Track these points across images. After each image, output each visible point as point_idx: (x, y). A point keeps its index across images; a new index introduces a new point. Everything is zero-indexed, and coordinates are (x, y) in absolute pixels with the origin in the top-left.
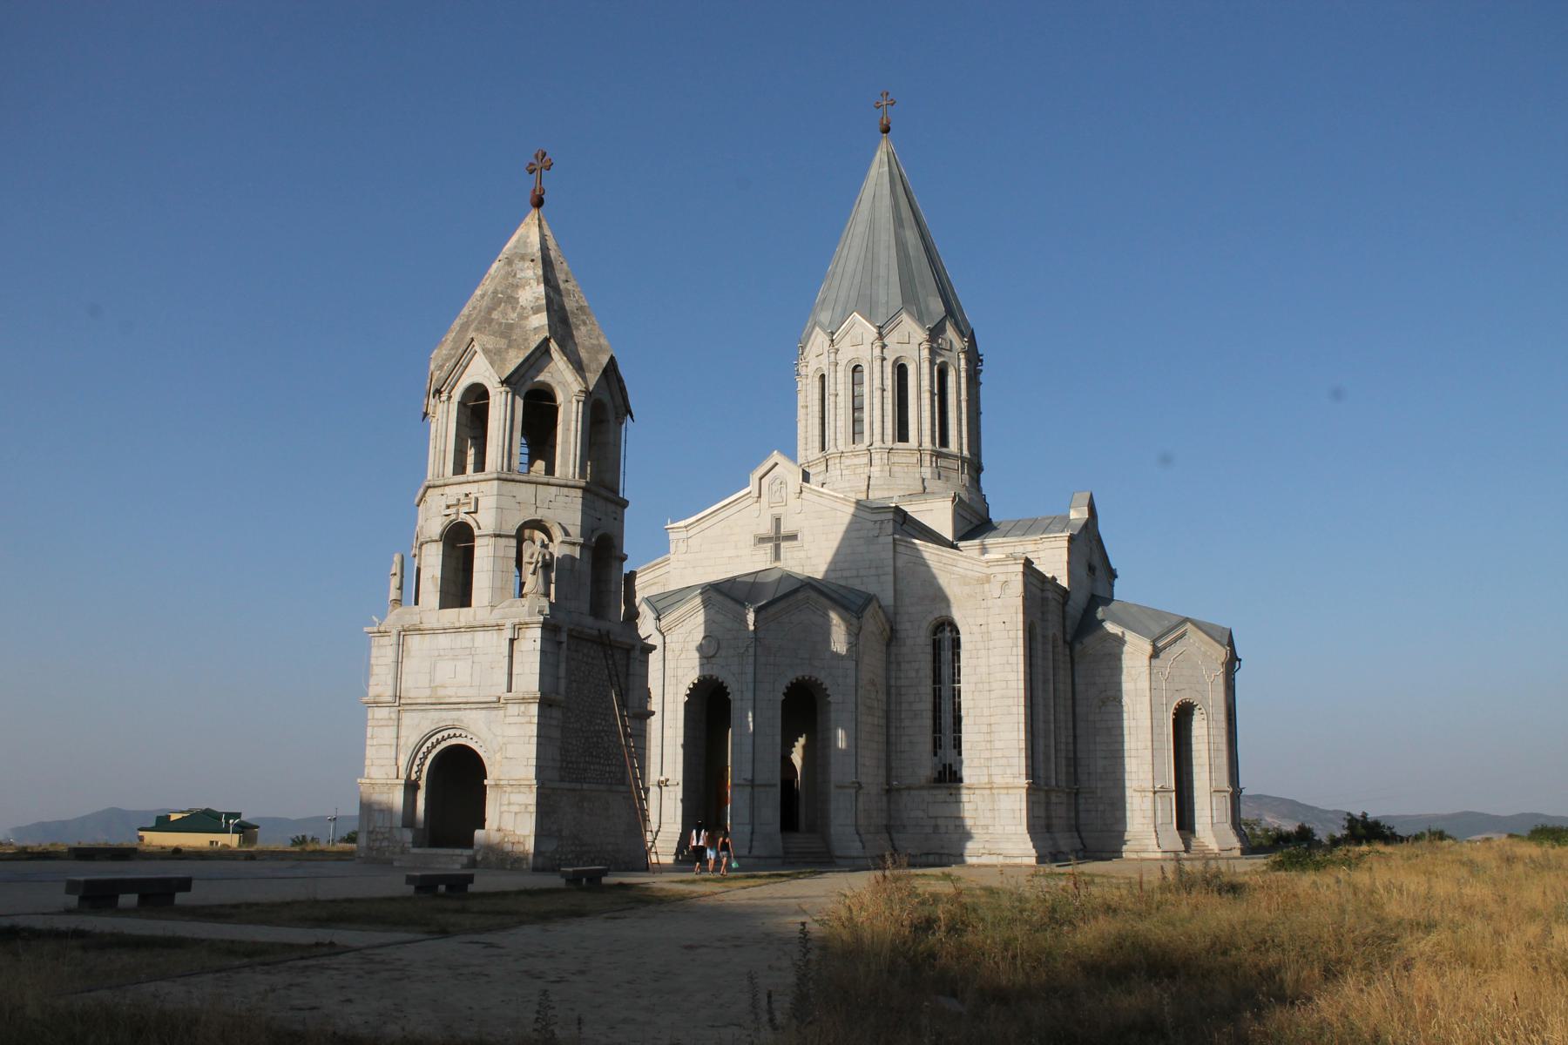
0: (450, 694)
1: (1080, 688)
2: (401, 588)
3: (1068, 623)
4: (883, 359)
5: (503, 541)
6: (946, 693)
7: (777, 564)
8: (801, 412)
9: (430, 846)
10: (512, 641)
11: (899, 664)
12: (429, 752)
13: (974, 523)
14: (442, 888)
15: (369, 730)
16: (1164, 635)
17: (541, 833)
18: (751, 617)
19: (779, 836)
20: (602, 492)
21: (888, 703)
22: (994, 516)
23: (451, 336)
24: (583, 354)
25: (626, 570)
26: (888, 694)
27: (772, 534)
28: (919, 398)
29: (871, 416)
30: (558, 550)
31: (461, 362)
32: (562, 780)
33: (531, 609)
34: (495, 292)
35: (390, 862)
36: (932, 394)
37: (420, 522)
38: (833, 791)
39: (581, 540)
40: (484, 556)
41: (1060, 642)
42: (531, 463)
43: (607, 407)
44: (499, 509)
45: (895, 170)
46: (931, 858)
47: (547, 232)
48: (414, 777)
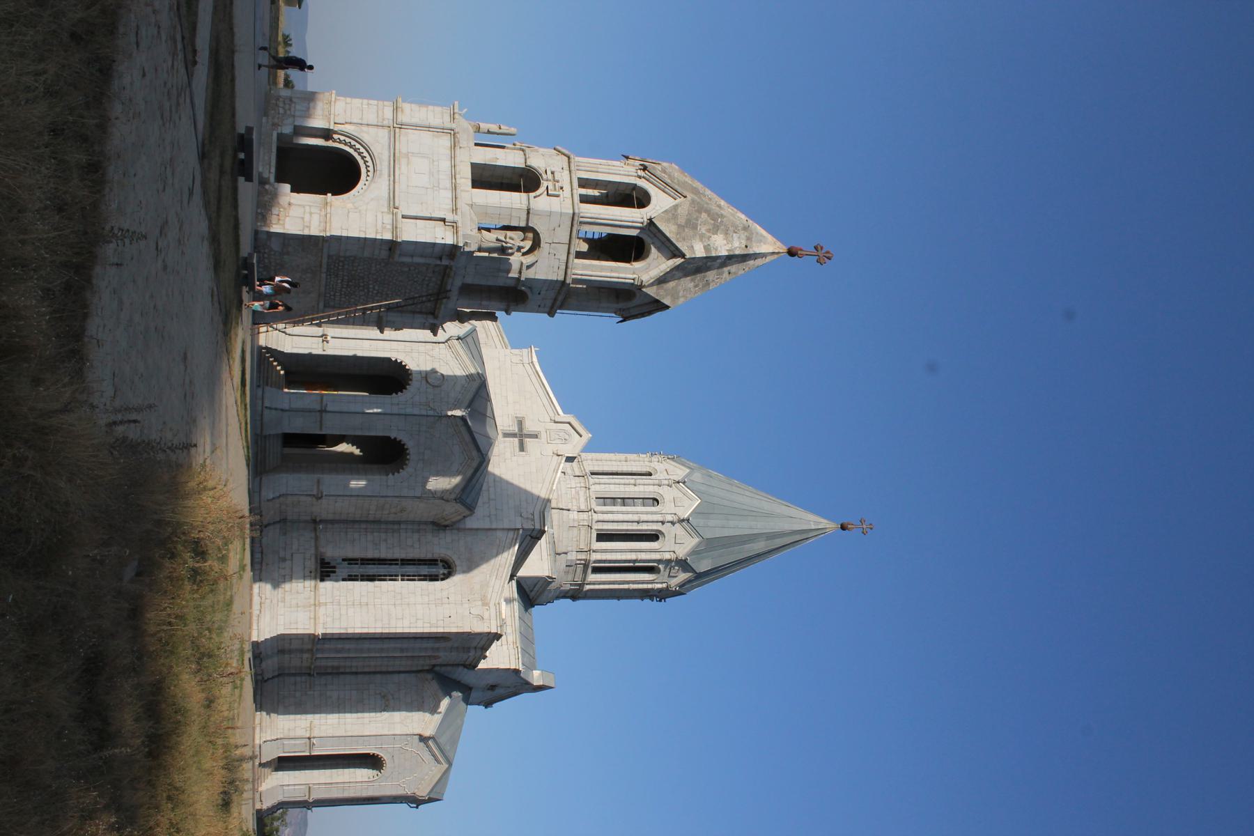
0: (402, 168)
1: (396, 677)
2: (489, 132)
3: (449, 668)
4: (663, 523)
5: (524, 216)
6: (393, 569)
7: (500, 435)
8: (622, 456)
9: (279, 150)
10: (443, 220)
11: (418, 531)
12: (355, 150)
13: (531, 594)
14: (242, 156)
15: (375, 102)
16: (438, 746)
17: (288, 240)
18: (458, 413)
19: (280, 432)
20: (562, 297)
21: (387, 522)
22: (536, 609)
23: (688, 180)
24: (671, 284)
25: (498, 314)
26: (393, 523)
27: (525, 432)
28: (631, 551)
29: (618, 512)
30: (516, 259)
31: (668, 187)
32: (329, 257)
33: (470, 237)
35: (266, 114)
36: (635, 561)
37: (542, 150)
39: (523, 279)
40: (512, 201)
41: (434, 662)
42: (586, 240)
43: (629, 302)
44: (550, 214)
45: (811, 534)
46: (258, 556)
47: (769, 259)
48: (336, 136)
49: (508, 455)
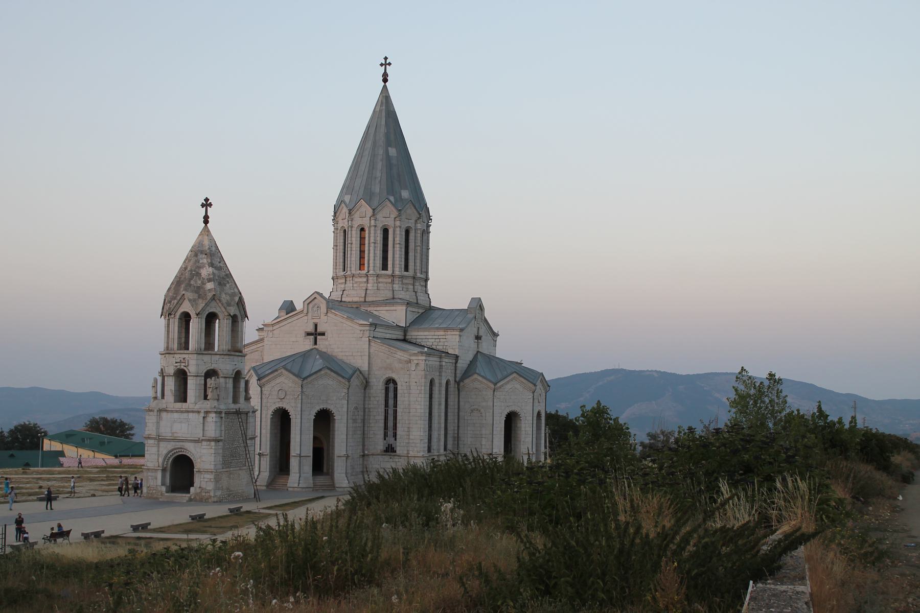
3: (458, 372)
6: (391, 412)
19: (311, 478)
26: (364, 411)
27: (313, 331)
31: (179, 304)
34: (191, 271)
40: (193, 385)
41: (452, 382)
49: (327, 343)
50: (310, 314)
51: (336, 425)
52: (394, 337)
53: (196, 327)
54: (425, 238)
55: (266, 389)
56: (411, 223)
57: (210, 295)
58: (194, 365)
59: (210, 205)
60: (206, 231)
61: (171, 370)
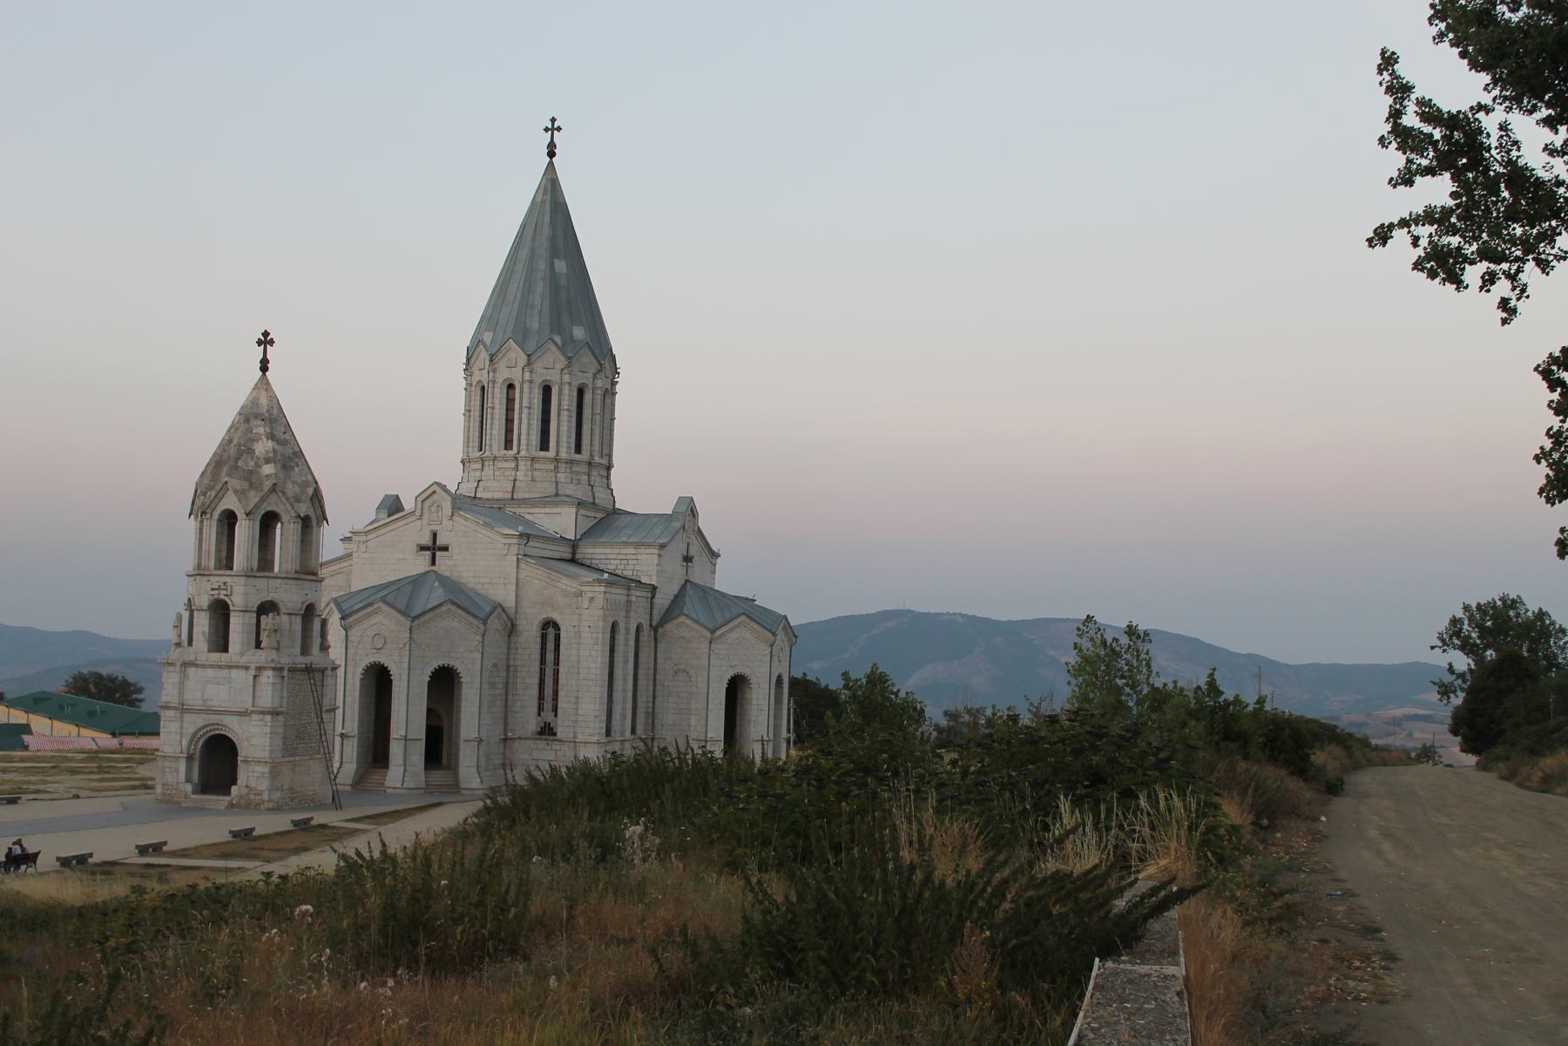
1: (660, 661)
3: (655, 611)
6: (549, 672)
26: (508, 671)
27: (430, 543)
31: (219, 497)
34: (239, 445)
38: (462, 745)
44: (246, 594)
49: (451, 563)
50: (426, 517)
51: (464, 691)
52: (557, 555)
53: (245, 532)
54: (608, 401)
55: (355, 634)
56: (587, 379)
57: (268, 485)
58: (241, 594)
59: (272, 342)
60: (264, 383)
61: (204, 601)
